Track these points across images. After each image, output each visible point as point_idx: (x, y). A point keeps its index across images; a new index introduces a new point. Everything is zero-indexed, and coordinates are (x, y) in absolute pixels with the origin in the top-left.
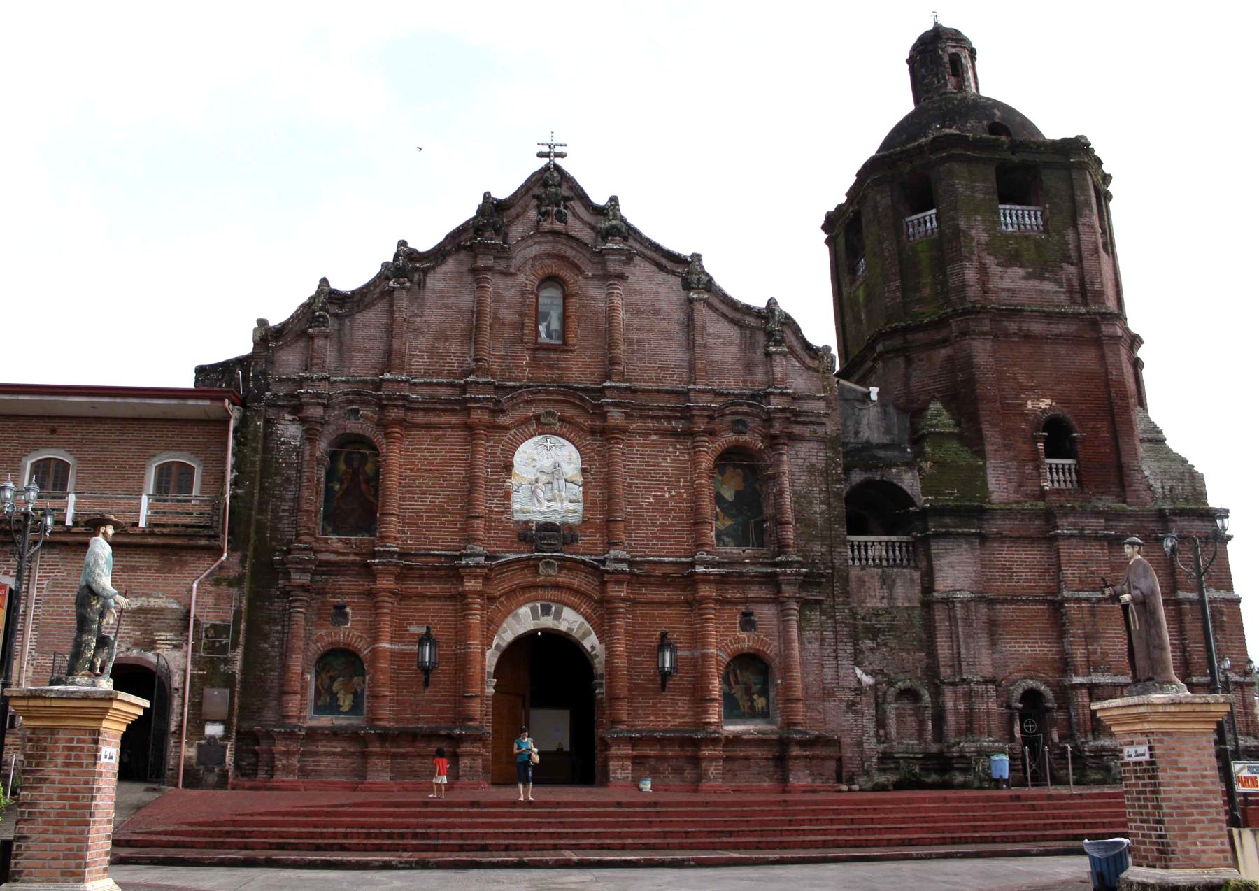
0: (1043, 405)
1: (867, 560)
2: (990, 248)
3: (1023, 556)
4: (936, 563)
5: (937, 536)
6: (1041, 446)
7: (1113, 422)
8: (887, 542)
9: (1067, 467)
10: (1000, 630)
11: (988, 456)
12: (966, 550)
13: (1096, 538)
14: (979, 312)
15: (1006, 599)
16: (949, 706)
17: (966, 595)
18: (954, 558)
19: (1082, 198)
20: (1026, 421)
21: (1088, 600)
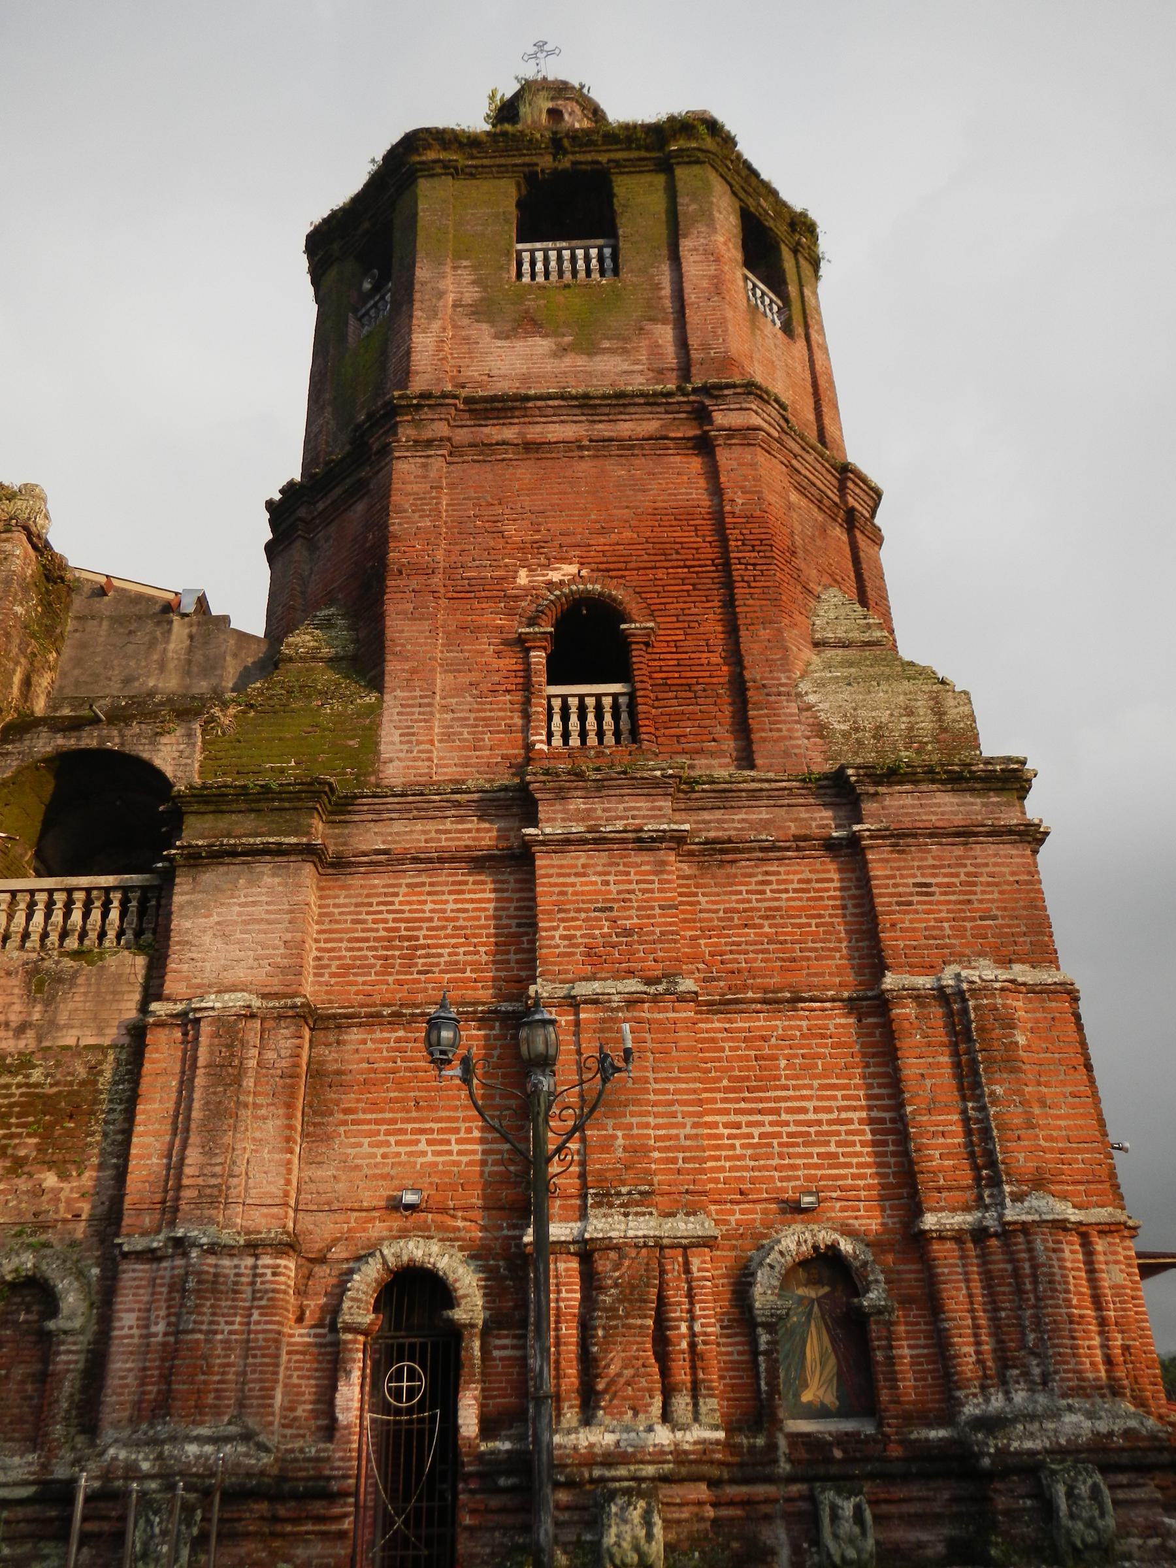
0: (555, 576)
1: (26, 935)
2: (482, 311)
3: (451, 906)
4: (181, 924)
5: (197, 859)
6: (538, 657)
7: (729, 604)
8: (88, 891)
9: (607, 702)
10: (349, 1099)
11: (389, 681)
12: (271, 890)
13: (643, 842)
14: (418, 407)
15: (379, 1015)
16: (127, 1321)
17: (236, 1000)
18: (233, 912)
19: (693, 207)
20: (510, 613)
21: (594, 1001)
